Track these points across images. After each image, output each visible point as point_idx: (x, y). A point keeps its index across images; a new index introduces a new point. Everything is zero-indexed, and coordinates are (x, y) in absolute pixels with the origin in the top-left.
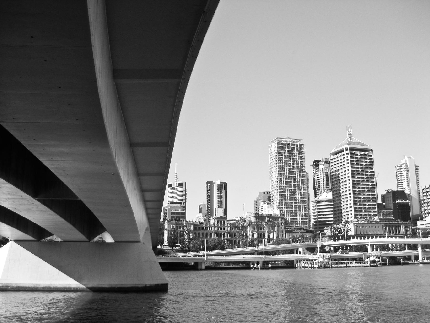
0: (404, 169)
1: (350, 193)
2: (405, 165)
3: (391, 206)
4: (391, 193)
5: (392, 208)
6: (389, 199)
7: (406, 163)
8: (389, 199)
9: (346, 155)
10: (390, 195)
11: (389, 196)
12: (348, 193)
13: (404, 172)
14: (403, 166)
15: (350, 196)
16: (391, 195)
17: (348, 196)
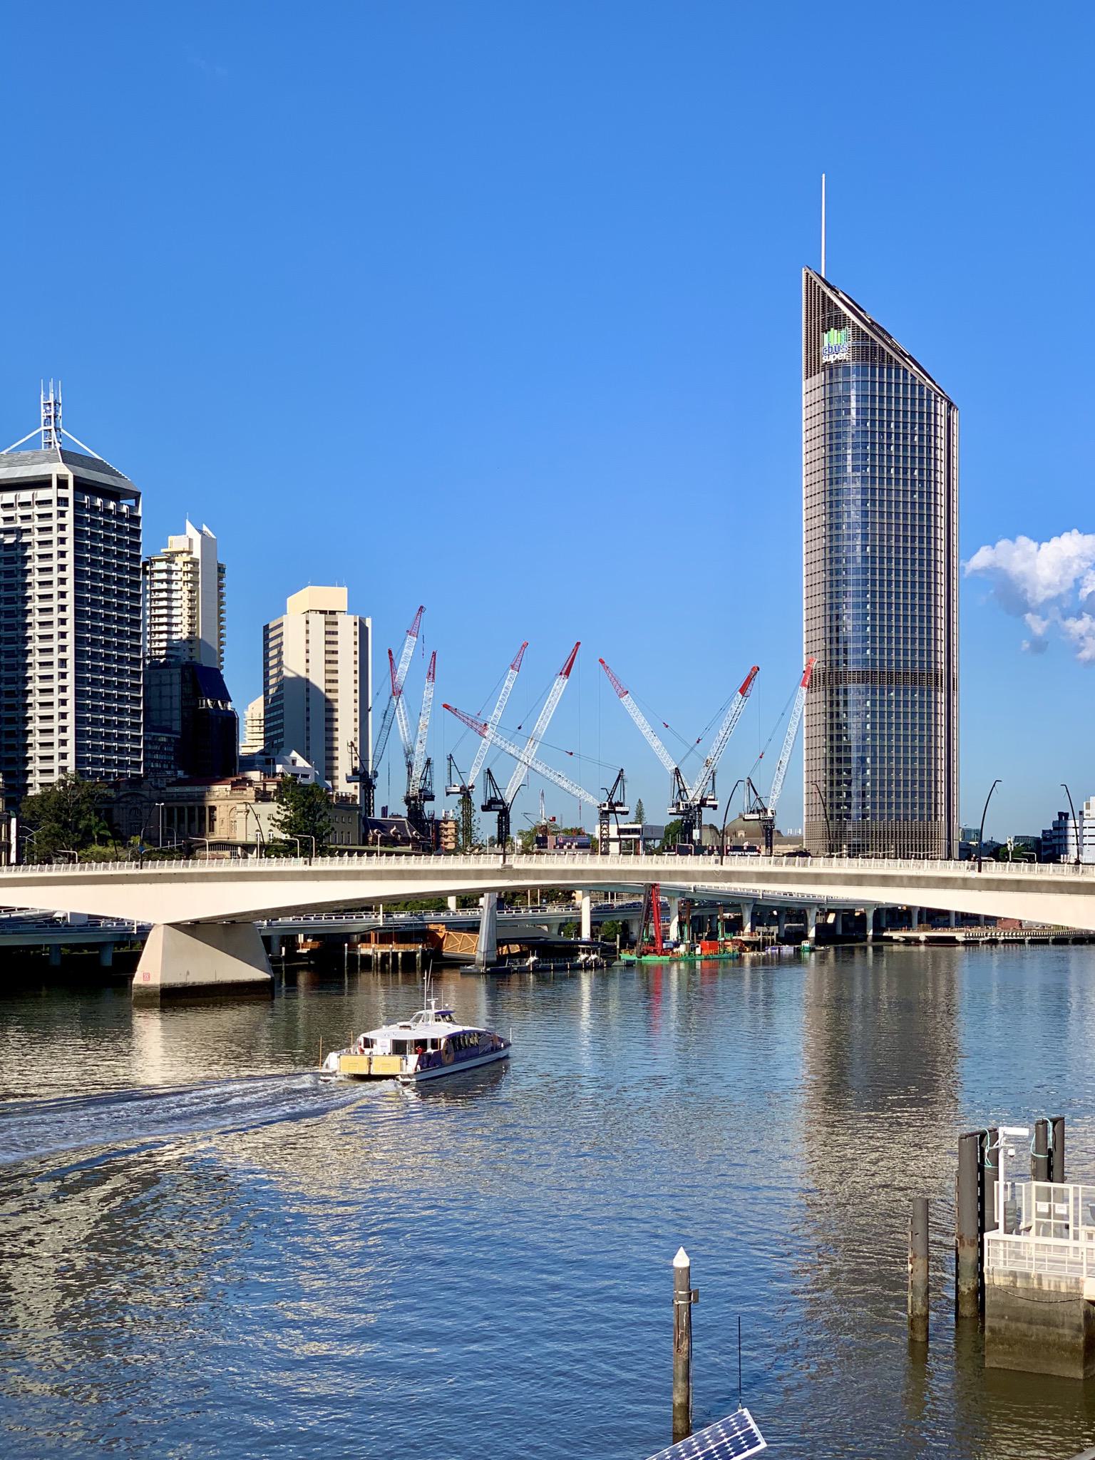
0: (180, 574)
1: (63, 662)
2: (186, 558)
3: (171, 720)
4: (179, 670)
5: (177, 726)
6: (166, 690)
7: (190, 553)
8: (166, 690)
9: (58, 505)
10: (171, 675)
11: (166, 679)
12: (55, 657)
13: (181, 584)
14: (179, 560)
15: (63, 670)
16: (177, 679)
17: (55, 670)
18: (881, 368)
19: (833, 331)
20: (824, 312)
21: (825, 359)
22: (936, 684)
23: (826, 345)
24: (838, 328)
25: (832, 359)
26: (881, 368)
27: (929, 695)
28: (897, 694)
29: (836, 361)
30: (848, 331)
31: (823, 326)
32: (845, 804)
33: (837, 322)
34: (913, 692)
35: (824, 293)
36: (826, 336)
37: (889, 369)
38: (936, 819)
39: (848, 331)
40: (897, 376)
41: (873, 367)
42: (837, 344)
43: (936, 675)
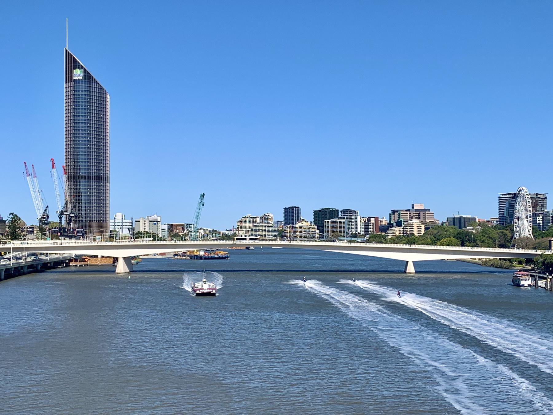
18: (92, 82)
19: (77, 70)
20: (74, 63)
21: (74, 78)
22: (105, 180)
23: (75, 73)
24: (79, 69)
25: (77, 78)
26: (92, 82)
27: (105, 184)
28: (97, 183)
29: (79, 79)
30: (82, 70)
31: (74, 67)
32: (81, 217)
33: (80, 67)
34: (101, 182)
35: (74, 58)
36: (75, 71)
37: (95, 83)
38: (105, 222)
39: (82, 70)
40: (97, 86)
41: (90, 82)
42: (78, 74)
43: (105, 177)
